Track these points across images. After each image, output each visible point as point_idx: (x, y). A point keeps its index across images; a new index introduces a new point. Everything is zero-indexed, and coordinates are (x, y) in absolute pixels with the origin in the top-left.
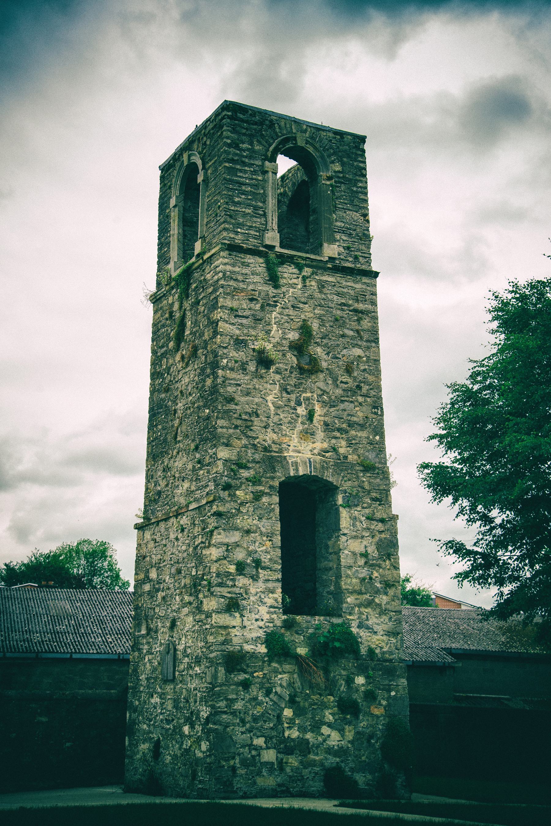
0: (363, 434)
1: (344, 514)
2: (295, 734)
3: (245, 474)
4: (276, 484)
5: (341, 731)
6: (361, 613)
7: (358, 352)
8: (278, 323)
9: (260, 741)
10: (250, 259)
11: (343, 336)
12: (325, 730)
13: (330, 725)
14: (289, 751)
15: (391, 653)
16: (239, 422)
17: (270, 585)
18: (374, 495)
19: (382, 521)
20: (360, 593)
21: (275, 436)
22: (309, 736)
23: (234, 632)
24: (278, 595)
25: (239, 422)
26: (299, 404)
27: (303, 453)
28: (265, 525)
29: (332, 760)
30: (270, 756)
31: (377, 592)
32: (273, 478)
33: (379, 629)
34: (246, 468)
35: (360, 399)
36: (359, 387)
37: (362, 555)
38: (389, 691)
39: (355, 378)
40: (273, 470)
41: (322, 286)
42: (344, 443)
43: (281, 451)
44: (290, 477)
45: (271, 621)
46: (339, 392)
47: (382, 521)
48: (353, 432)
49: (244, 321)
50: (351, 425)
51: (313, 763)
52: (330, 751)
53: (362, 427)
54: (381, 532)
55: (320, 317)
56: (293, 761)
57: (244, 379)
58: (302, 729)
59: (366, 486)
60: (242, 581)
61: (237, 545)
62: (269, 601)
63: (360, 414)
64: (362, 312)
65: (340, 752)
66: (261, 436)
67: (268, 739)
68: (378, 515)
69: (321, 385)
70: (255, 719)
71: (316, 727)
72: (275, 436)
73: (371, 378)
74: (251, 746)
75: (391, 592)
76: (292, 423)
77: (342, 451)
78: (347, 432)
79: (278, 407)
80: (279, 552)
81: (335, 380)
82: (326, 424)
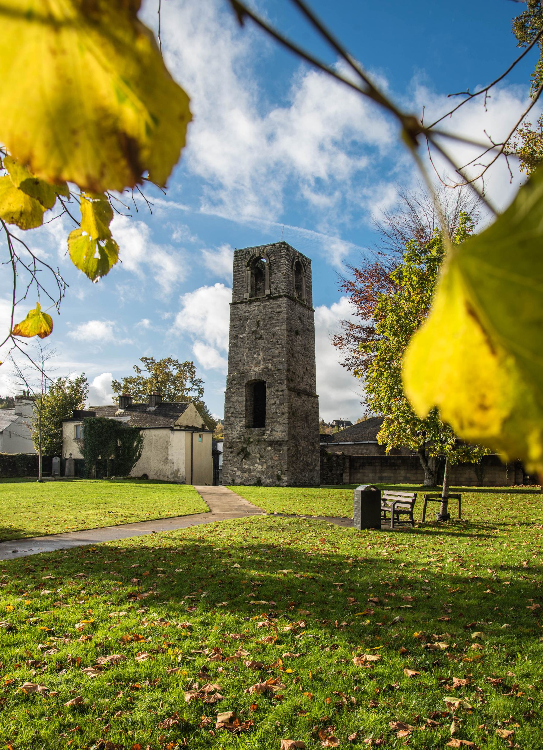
0: (278, 359)
1: (268, 391)
2: (247, 467)
3: (234, 382)
4: (244, 384)
5: (262, 465)
6: (272, 425)
7: (277, 328)
8: (249, 326)
9: (236, 469)
10: (239, 306)
11: (273, 323)
12: (256, 465)
13: (258, 464)
14: (245, 472)
15: (282, 438)
16: (235, 365)
17: (241, 419)
18: (279, 382)
19: (282, 391)
20: (272, 418)
21: (246, 367)
22: (251, 467)
23: (229, 436)
24: (244, 422)
25: (235, 365)
26: (255, 353)
27: (254, 371)
28: (240, 399)
29: (258, 475)
30: (239, 473)
31: (279, 417)
32: (243, 383)
33: (279, 430)
34: (234, 380)
35: (277, 346)
36: (277, 342)
37: (273, 404)
38: (280, 451)
39: (276, 339)
40: (243, 380)
41: (264, 307)
42: (270, 364)
43: (248, 372)
44: (248, 381)
45: (241, 431)
46: (269, 345)
47: (282, 391)
48: (274, 360)
49: (237, 329)
50: (273, 357)
51: (253, 476)
52: (258, 472)
53: (278, 356)
54: (281, 395)
55: (264, 319)
56: (246, 475)
57: (236, 349)
58: (249, 465)
59: (276, 379)
60: (232, 419)
61: (231, 407)
62: (241, 424)
63: (277, 352)
64: (279, 312)
65: (262, 472)
66: (242, 368)
67: (238, 468)
68: (280, 389)
69: (263, 344)
70: (234, 462)
71: (253, 465)
72: (246, 367)
73: (282, 337)
74: (233, 470)
75: (284, 416)
76: (252, 361)
77: (269, 367)
78: (272, 360)
79: (247, 356)
80: (244, 408)
81: (268, 341)
82: (264, 359)
